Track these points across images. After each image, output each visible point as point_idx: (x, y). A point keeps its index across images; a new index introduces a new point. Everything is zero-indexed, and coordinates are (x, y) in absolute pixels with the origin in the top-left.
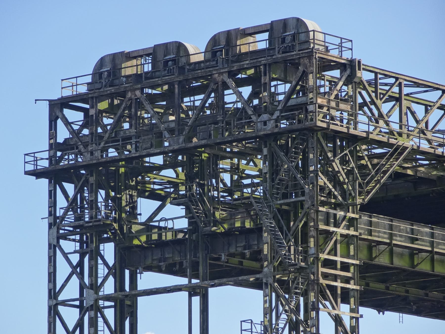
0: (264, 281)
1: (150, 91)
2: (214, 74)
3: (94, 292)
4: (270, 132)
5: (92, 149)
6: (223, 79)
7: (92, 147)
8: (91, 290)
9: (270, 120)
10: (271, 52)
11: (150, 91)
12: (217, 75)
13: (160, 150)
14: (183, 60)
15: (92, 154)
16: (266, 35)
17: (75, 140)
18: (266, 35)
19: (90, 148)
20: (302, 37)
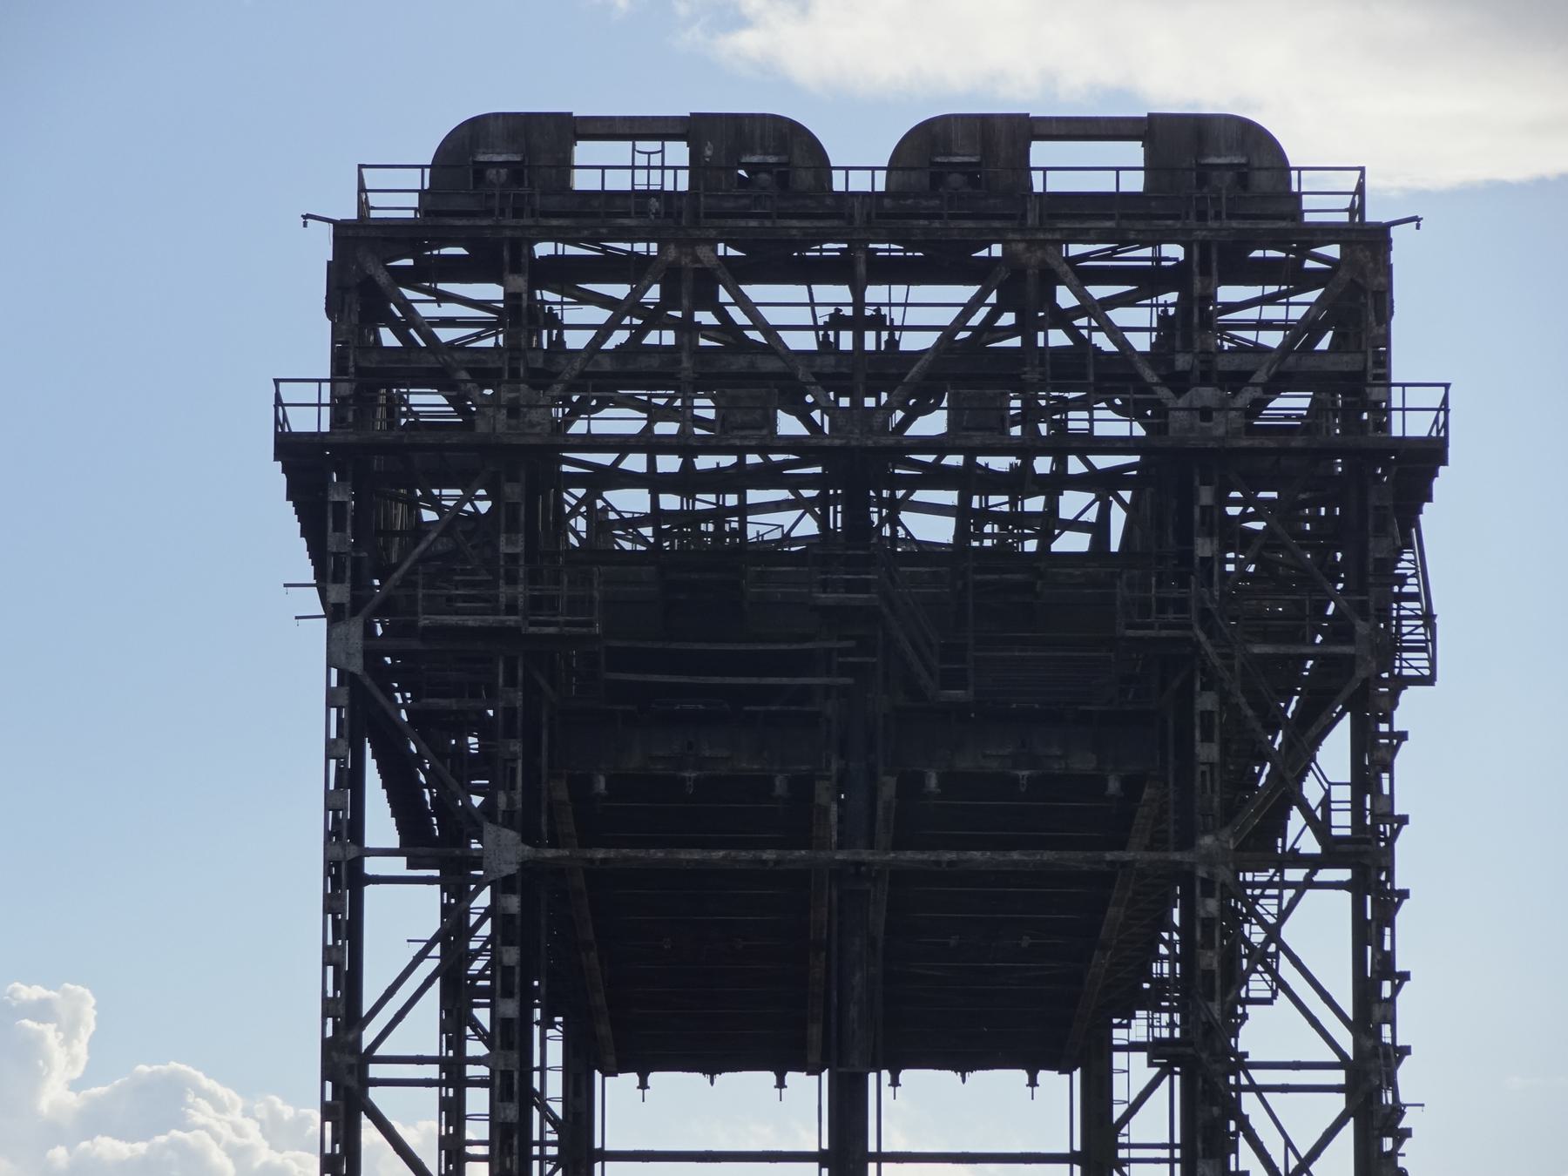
0: (1201, 872)
1: (640, 247)
2: (1014, 241)
3: (519, 838)
4: (1276, 446)
5: (516, 399)
6: (1043, 261)
7: (518, 390)
8: (506, 831)
9: (1224, 408)
10: (1153, 204)
11: (640, 247)
12: (1021, 246)
13: (844, 441)
14: (804, 179)
15: (514, 410)
16: (1133, 152)
17: (444, 359)
18: (1133, 152)
19: (506, 395)
20: (1262, 181)
